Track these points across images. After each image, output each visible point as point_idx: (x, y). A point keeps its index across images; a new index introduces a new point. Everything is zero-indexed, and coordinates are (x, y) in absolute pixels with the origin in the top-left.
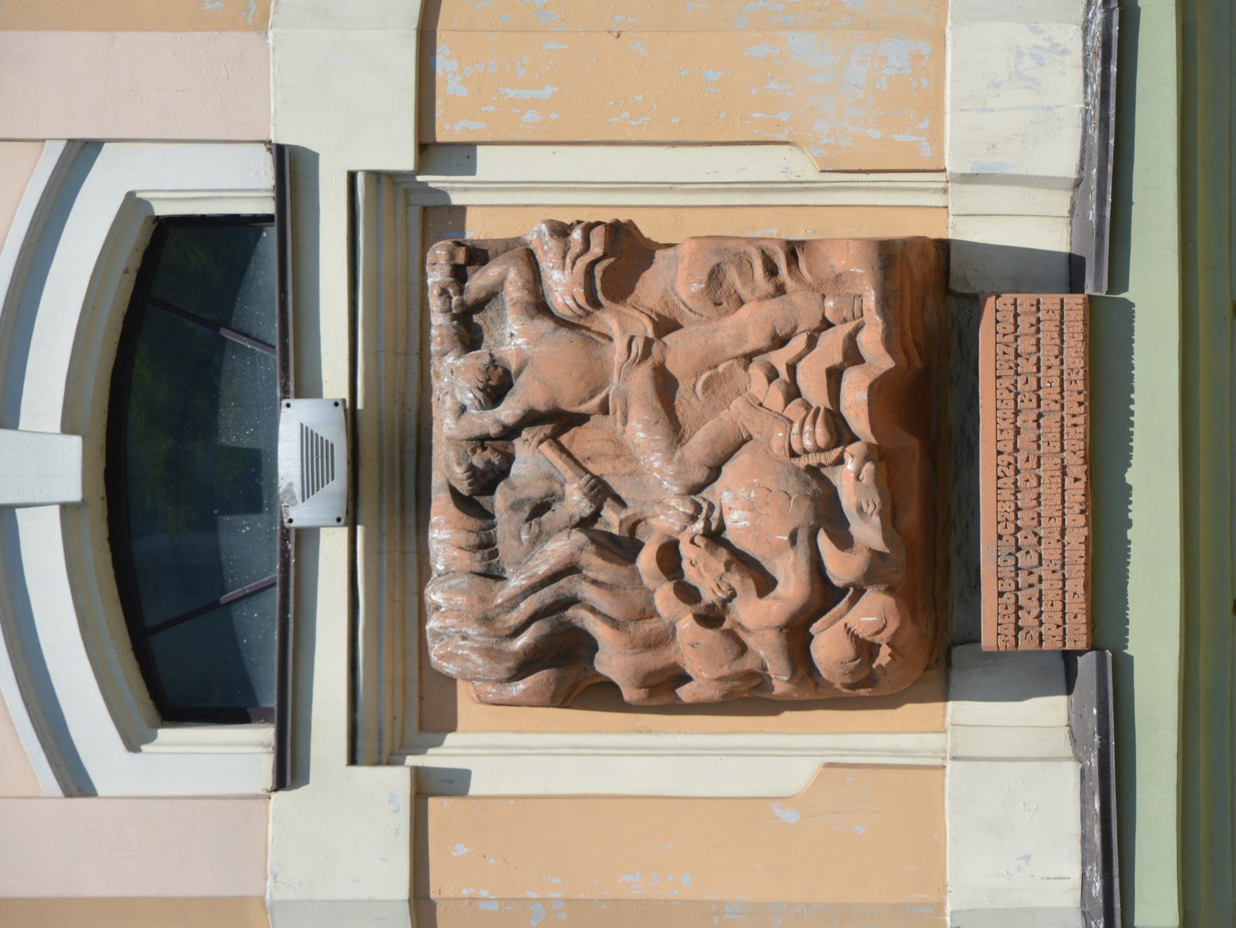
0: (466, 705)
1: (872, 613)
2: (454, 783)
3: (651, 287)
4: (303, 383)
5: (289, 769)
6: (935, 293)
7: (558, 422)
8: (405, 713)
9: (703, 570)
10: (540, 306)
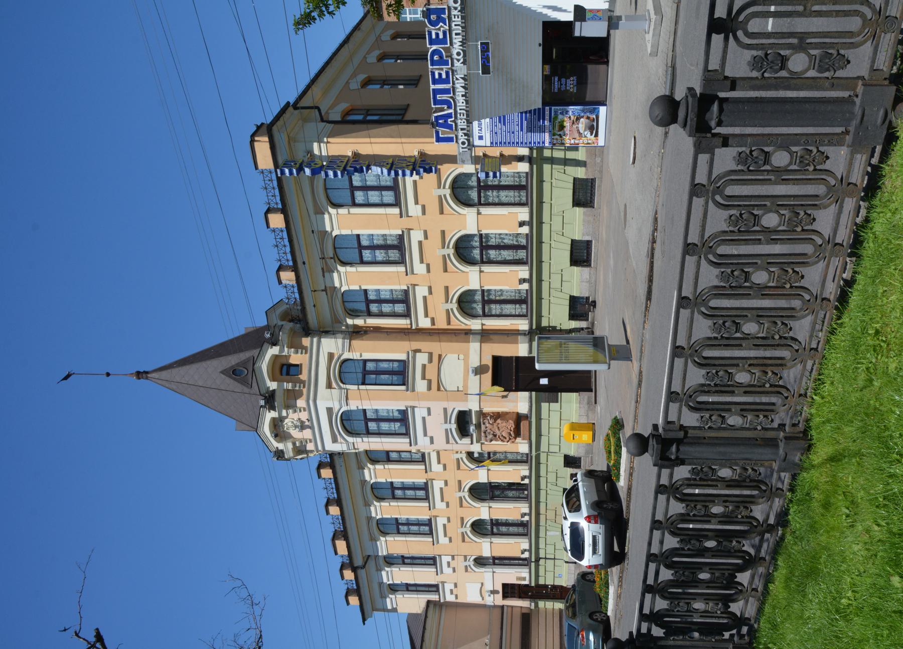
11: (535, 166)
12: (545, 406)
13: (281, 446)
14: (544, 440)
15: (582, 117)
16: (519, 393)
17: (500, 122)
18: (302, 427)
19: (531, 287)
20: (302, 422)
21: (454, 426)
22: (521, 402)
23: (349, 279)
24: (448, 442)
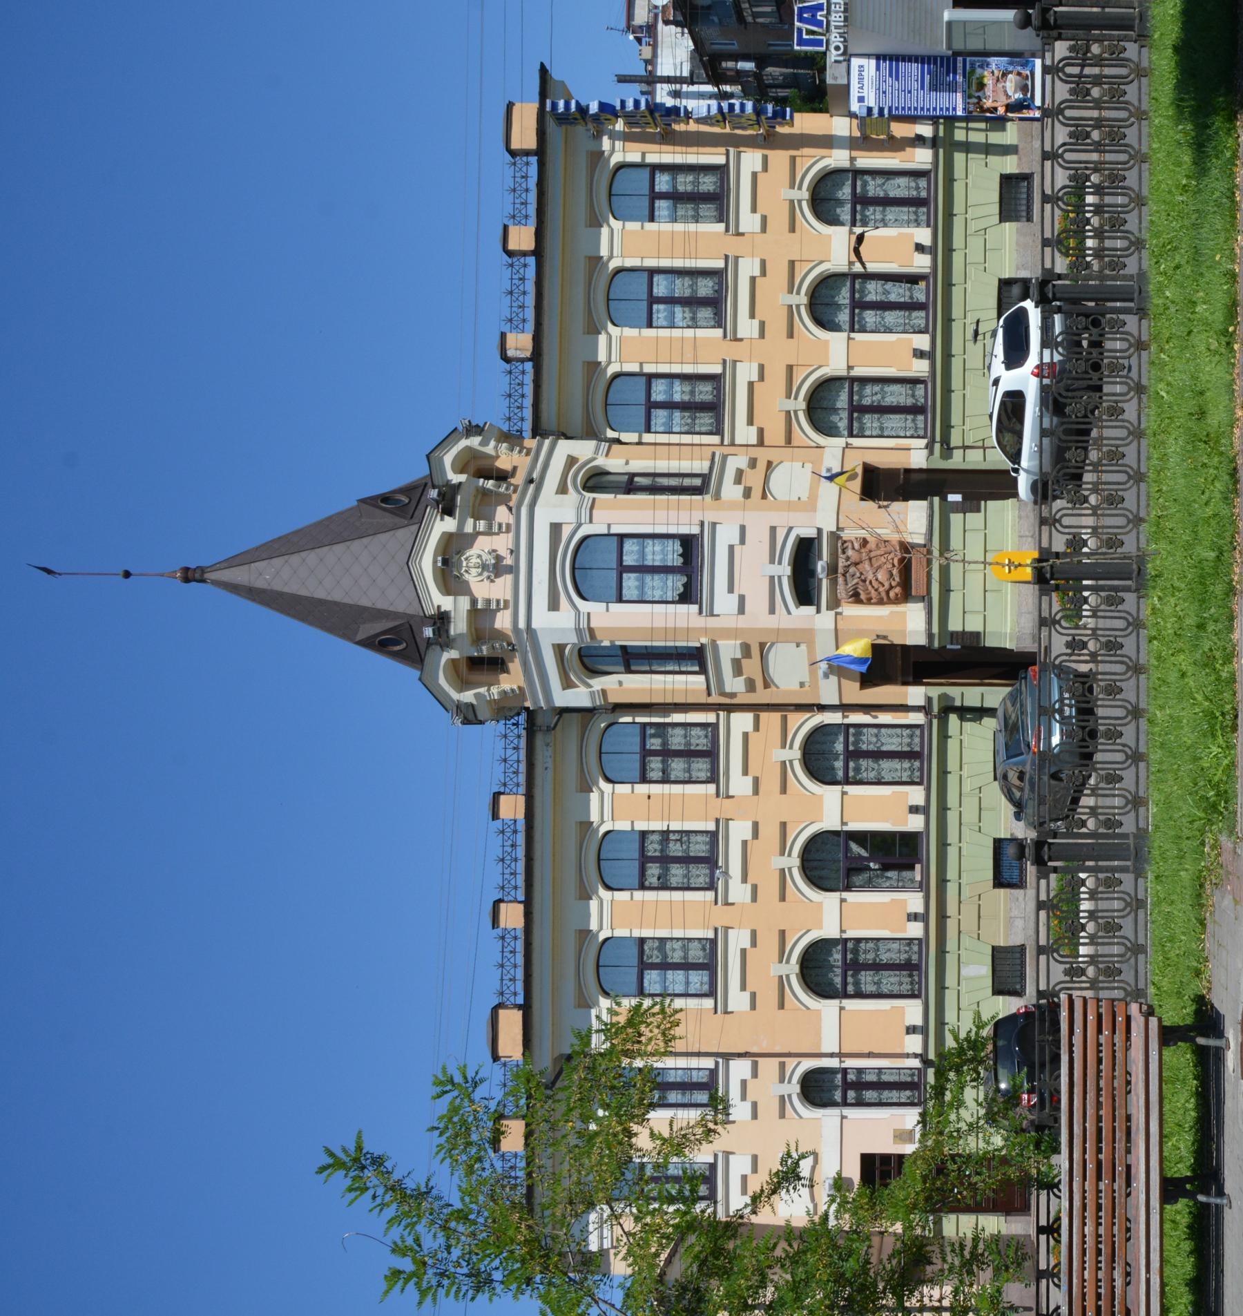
0: (843, 603)
1: (898, 590)
2: (841, 614)
3: (868, 546)
4: (820, 558)
5: (818, 611)
6: (905, 547)
7: (856, 564)
8: (834, 604)
9: (875, 584)
10: (853, 548)
11: (941, 151)
12: (956, 519)
13: (446, 603)
14: (955, 599)
15: (1011, 72)
16: (911, 503)
17: (891, 75)
18: (497, 568)
19: (935, 260)
20: (499, 558)
21: (785, 570)
22: (912, 519)
23: (624, 348)
24: (772, 611)
